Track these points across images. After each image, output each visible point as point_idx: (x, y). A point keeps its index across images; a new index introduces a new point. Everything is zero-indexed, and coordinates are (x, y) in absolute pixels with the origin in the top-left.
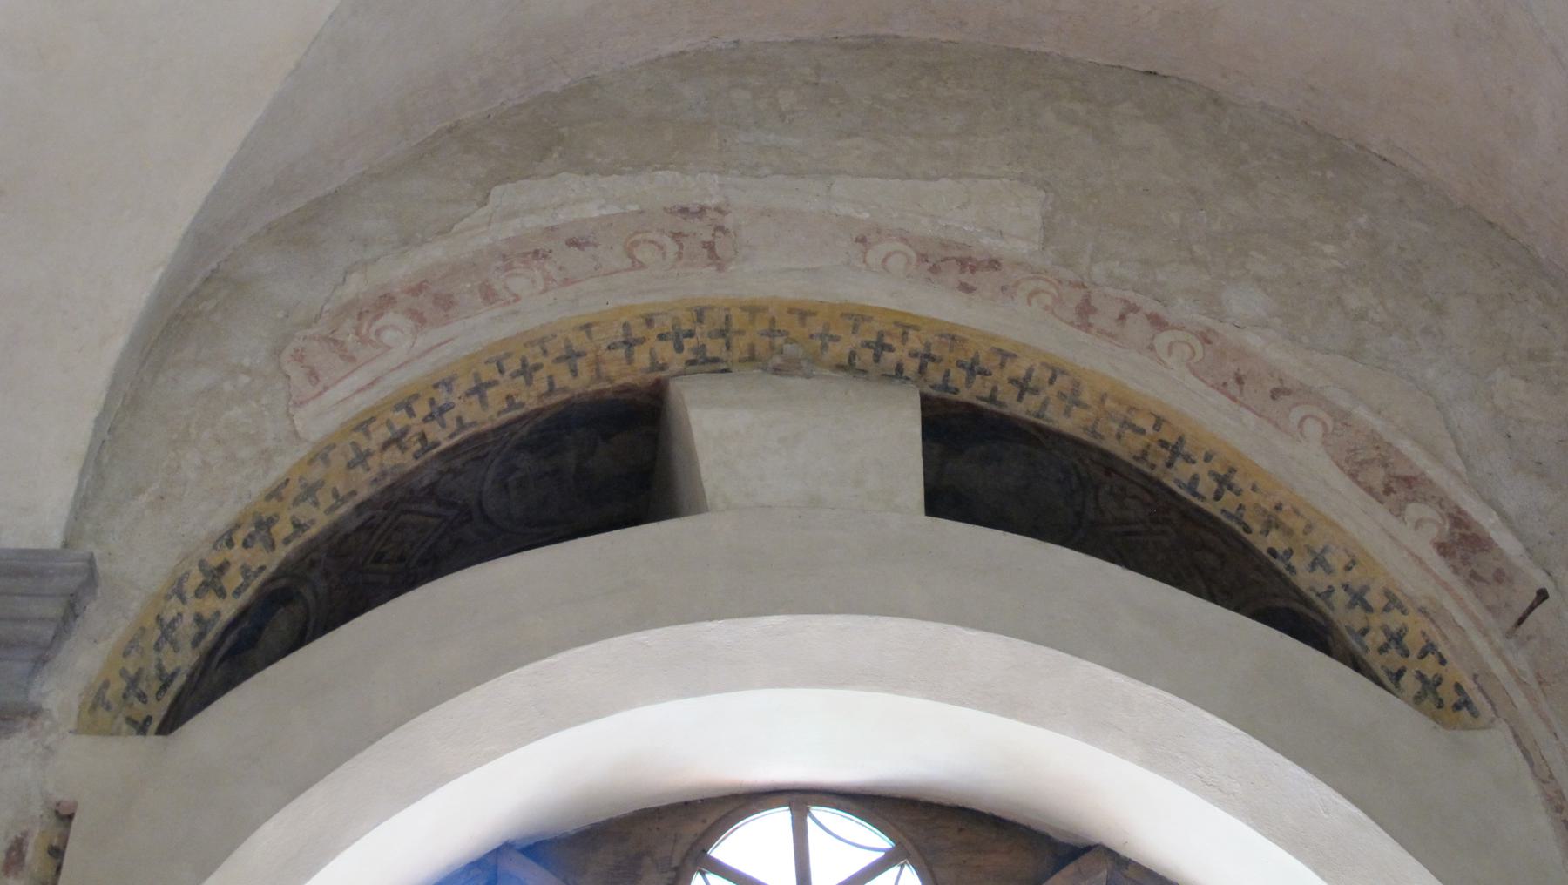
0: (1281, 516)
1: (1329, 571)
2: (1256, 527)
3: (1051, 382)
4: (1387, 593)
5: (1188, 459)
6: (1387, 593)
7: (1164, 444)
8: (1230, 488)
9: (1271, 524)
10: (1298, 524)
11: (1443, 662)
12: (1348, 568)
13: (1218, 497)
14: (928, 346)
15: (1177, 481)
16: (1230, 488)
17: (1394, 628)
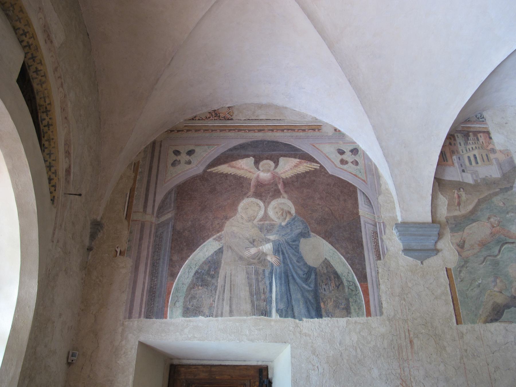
0: (51, 141)
1: (50, 157)
2: (46, 138)
3: (42, 76)
4: (56, 171)
5: (47, 115)
6: (56, 171)
7: (46, 108)
8: (49, 127)
9: (49, 140)
10: (53, 145)
11: (55, 190)
12: (53, 160)
13: (45, 126)
14: (32, 44)
15: (41, 116)
16: (49, 127)
17: (52, 177)
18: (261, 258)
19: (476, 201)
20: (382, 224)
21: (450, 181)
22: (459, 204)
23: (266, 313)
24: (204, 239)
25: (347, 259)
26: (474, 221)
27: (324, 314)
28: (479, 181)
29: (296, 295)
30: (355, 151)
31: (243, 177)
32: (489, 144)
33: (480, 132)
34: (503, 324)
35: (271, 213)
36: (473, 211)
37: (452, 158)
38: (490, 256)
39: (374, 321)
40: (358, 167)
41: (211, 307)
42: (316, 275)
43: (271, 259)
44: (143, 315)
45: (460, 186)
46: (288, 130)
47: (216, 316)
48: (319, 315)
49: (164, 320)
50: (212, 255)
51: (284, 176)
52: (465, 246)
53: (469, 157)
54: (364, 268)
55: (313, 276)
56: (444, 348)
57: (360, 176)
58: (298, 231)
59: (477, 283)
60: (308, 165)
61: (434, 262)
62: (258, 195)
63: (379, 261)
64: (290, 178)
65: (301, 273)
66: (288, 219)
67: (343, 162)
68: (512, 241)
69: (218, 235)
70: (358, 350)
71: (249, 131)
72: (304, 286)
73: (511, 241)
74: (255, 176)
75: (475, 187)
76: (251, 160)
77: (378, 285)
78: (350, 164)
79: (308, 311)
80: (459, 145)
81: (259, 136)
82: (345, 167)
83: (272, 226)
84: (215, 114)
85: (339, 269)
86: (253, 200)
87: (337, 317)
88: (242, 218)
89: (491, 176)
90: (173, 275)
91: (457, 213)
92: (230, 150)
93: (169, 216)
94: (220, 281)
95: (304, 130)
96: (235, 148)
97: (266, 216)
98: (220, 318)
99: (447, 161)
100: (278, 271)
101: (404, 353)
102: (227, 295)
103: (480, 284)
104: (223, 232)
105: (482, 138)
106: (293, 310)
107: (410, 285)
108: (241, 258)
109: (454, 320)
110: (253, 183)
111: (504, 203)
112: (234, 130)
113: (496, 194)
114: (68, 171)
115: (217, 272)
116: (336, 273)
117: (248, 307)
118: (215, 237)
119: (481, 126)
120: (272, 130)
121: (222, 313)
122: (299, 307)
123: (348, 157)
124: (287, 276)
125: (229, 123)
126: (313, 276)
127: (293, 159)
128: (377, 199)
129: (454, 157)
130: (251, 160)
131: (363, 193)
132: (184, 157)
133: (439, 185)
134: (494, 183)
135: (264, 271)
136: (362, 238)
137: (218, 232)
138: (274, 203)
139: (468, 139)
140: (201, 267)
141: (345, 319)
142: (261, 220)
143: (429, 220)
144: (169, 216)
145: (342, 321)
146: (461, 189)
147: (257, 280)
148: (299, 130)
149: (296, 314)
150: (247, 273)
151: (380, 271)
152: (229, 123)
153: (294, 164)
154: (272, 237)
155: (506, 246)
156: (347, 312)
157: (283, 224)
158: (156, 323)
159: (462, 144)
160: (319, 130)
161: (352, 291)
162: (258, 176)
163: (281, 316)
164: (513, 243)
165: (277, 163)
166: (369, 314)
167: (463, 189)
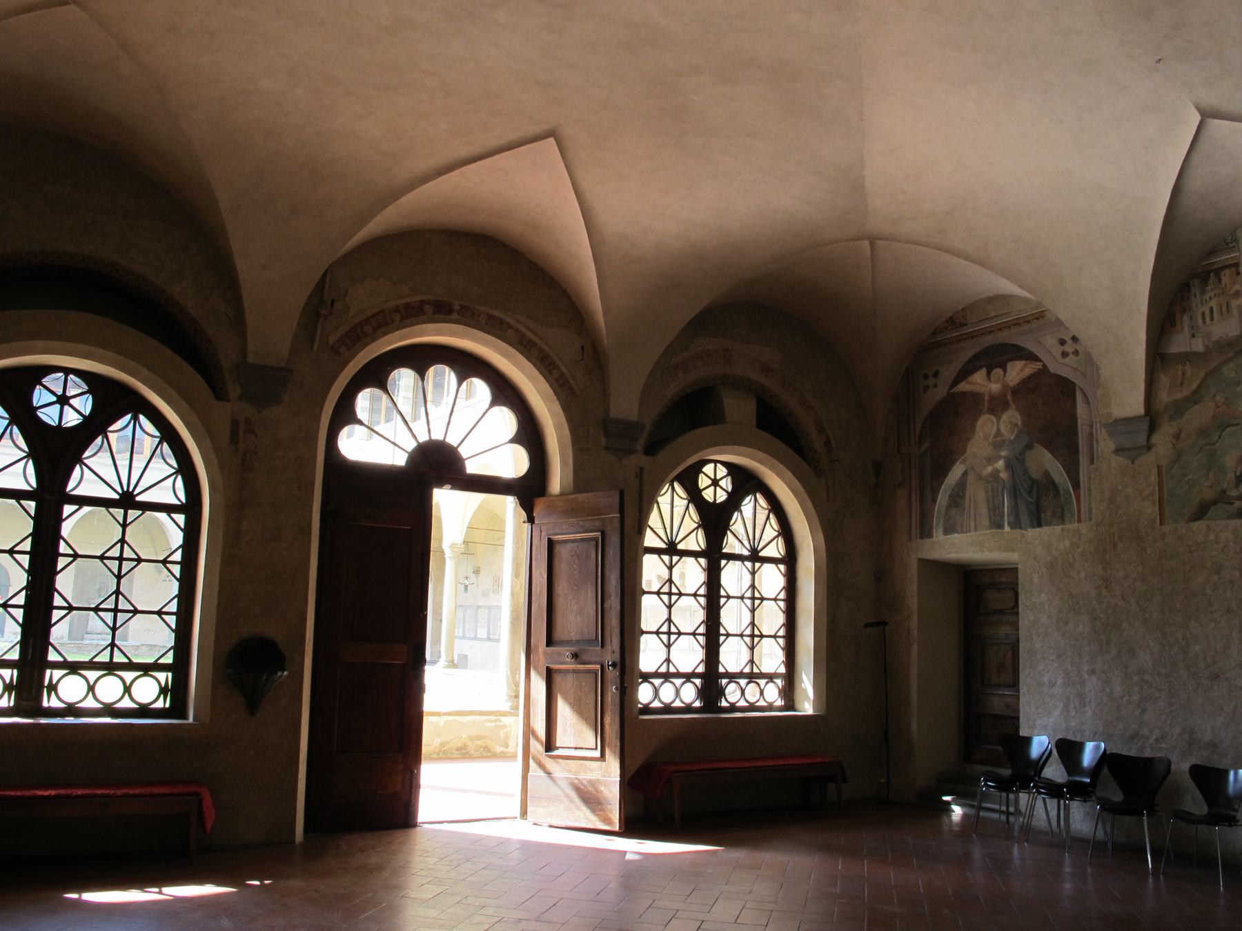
18: (995, 475)
19: (1202, 375)
20: (1098, 423)
21: (1175, 354)
22: (1182, 383)
23: (1000, 526)
24: (953, 463)
25: (1064, 467)
26: (1196, 403)
27: (1043, 523)
28: (1211, 346)
29: (1022, 508)
30: (1074, 339)
31: (978, 393)
32: (1234, 284)
33: (1224, 268)
34: (1206, 522)
35: (1003, 430)
36: (1197, 391)
37: (1182, 318)
38: (1207, 445)
39: (1084, 527)
40: (1078, 358)
41: (962, 526)
42: (1038, 485)
43: (1003, 475)
44: (918, 537)
45: (1186, 357)
46: (1015, 325)
47: (966, 532)
48: (1040, 525)
49: (931, 540)
50: (960, 478)
51: (1011, 384)
52: (1181, 437)
53: (1203, 313)
54: (1078, 474)
55: (1035, 488)
56: (1145, 550)
57: (1080, 369)
58: (1023, 444)
59: (1187, 479)
60: (1033, 366)
61: (1149, 459)
62: (992, 411)
63: (1092, 466)
64: (1018, 385)
65: (1026, 486)
66: (1015, 433)
67: (1065, 354)
68: (1236, 422)
69: (963, 457)
70: (1070, 556)
71: (981, 335)
72: (1029, 499)
73: (1236, 422)
74: (988, 389)
75: (1205, 356)
76: (983, 371)
77: (1090, 490)
78: (1071, 355)
79: (1032, 522)
80: (1193, 298)
81: (989, 340)
82: (1067, 360)
83: (1003, 441)
84: (953, 322)
85: (1057, 479)
86: (986, 416)
87: (1055, 525)
88: (980, 437)
89: (1227, 335)
90: (935, 500)
91: (1179, 396)
92: (967, 363)
93: (926, 445)
94: (967, 501)
95: (1029, 322)
96: (970, 361)
97: (998, 433)
98: (969, 534)
99: (1175, 326)
100: (1008, 487)
101: (1108, 557)
102: (972, 513)
103: (1190, 479)
104: (966, 455)
105: (1226, 276)
106: (1020, 522)
107: (1120, 487)
108: (981, 478)
109: (1158, 521)
110: (986, 397)
111: (1237, 373)
112: (968, 338)
113: (1227, 361)
114: (827, 443)
115: (964, 493)
116: (1053, 483)
117: (986, 522)
118: (961, 460)
119: (1228, 257)
120: (1000, 330)
121: (970, 529)
122: (1025, 519)
123: (1069, 348)
124: (1015, 491)
125: (965, 330)
126: (1035, 488)
127: (1018, 362)
128: (1095, 394)
129: (1185, 318)
130: (983, 371)
131: (1082, 390)
132: (931, 381)
133: (1162, 362)
134: (1229, 345)
135: (998, 488)
136: (1078, 441)
137: (963, 454)
138: (1005, 417)
139: (1207, 284)
140: (953, 490)
141: (1060, 527)
142: (993, 438)
143: (1141, 411)
144: (926, 445)
145: (1058, 529)
146: (1188, 363)
147: (993, 498)
148: (1024, 322)
149: (1023, 525)
150: (986, 491)
151: (1092, 476)
152: (965, 330)
153: (1020, 368)
154: (1003, 453)
155: (1228, 429)
156: (1062, 520)
157: (1012, 438)
158: (927, 542)
159: (1198, 296)
160: (1043, 317)
161: (1067, 499)
162: (990, 388)
163: (1011, 528)
164: (1237, 424)
165: (1005, 370)
166: (1079, 521)
167: (1190, 362)
